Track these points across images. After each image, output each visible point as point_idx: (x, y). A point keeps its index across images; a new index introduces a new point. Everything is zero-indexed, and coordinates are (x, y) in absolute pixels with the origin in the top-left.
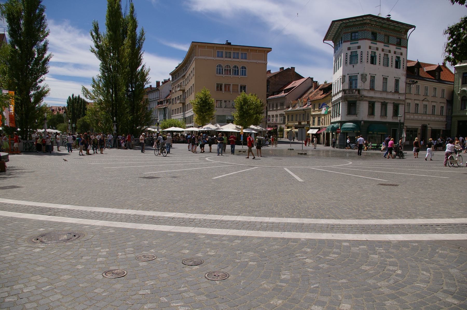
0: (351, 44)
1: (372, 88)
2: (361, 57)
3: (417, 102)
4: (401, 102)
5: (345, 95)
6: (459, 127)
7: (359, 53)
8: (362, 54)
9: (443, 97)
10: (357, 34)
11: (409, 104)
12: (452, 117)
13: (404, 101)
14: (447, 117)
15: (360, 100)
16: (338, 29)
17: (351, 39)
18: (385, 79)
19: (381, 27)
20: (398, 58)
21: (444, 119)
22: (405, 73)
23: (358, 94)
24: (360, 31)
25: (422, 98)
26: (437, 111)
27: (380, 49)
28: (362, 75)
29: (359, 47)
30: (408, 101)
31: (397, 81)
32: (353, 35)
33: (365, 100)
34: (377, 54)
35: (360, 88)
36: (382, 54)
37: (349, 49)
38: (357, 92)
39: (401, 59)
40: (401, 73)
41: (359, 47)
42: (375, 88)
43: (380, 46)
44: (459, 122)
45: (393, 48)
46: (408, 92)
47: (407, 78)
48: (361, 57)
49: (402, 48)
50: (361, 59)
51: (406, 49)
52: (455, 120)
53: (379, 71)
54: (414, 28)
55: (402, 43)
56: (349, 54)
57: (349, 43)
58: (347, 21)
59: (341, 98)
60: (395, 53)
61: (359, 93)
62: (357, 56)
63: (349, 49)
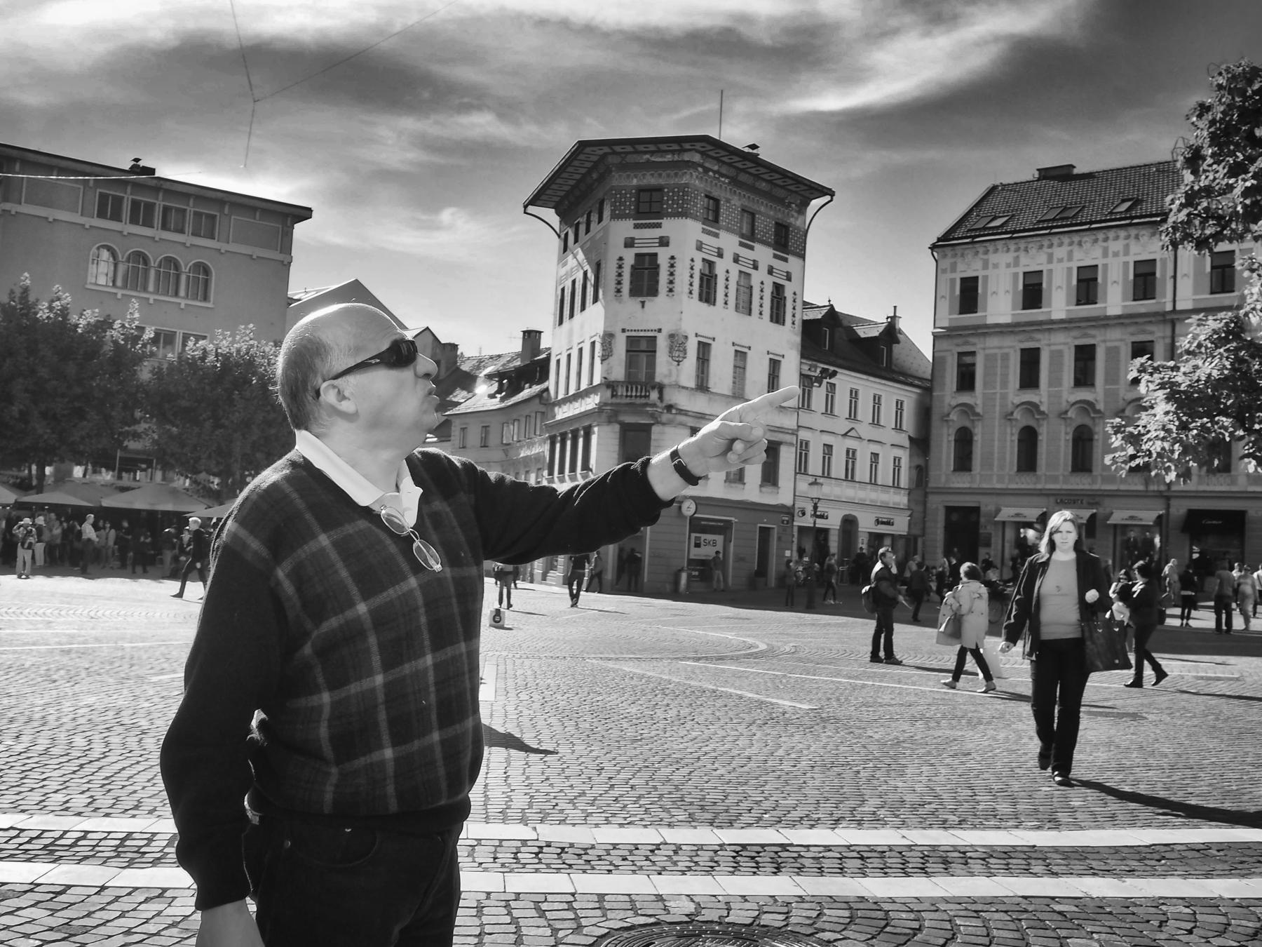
0: (636, 226)
1: (702, 386)
2: (672, 274)
3: (828, 439)
4: (788, 438)
5: (615, 400)
6: (950, 528)
7: (663, 261)
8: (672, 266)
9: (898, 428)
11: (807, 443)
12: (926, 495)
13: (794, 433)
14: (910, 492)
15: (664, 424)
16: (590, 171)
17: (638, 212)
18: (741, 356)
19: (734, 182)
20: (778, 288)
21: (902, 499)
22: (798, 339)
23: (659, 403)
25: (842, 425)
26: (885, 475)
27: (728, 256)
30: (803, 435)
31: (775, 365)
33: (682, 424)
34: (720, 270)
35: (666, 381)
36: (735, 270)
37: (629, 243)
38: (654, 395)
39: (788, 294)
40: (785, 341)
41: (664, 242)
42: (711, 384)
43: (729, 242)
44: (950, 510)
45: (764, 254)
46: (805, 402)
47: (803, 356)
48: (672, 274)
49: (791, 258)
50: (671, 282)
51: (800, 261)
52: (937, 504)
53: (720, 324)
54: (828, 198)
55: (788, 242)
56: (629, 260)
57: (631, 222)
58: (629, 148)
59: (600, 409)
60: (771, 271)
61: (661, 398)
62: (655, 268)
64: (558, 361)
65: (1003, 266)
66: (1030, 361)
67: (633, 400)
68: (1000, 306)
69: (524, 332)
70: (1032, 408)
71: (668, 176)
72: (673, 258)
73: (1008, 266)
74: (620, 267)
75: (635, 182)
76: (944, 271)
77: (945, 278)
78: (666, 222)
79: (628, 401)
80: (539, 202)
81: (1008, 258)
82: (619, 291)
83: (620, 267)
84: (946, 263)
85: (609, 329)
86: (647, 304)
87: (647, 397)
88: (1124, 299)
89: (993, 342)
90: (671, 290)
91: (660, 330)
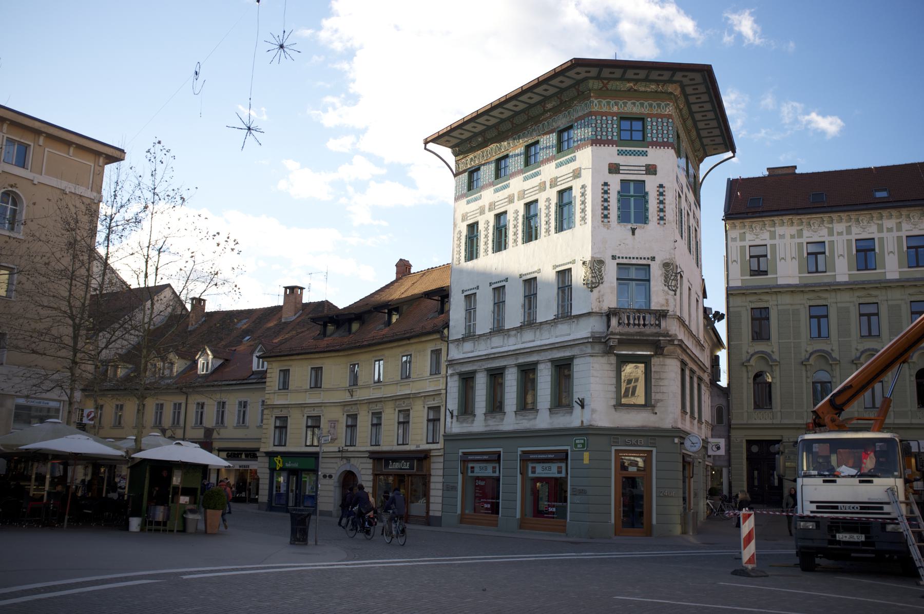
0: (620, 153)
2: (661, 202)
8: (661, 194)
10: (637, 125)
12: (729, 432)
24: (651, 116)
28: (666, 265)
29: (651, 170)
32: (626, 125)
37: (614, 169)
41: (651, 170)
44: (750, 443)
48: (661, 202)
52: (740, 437)
54: (730, 154)
57: (614, 150)
59: (596, 340)
62: (643, 197)
63: (614, 169)
64: (470, 298)
65: (788, 236)
66: (819, 316)
67: (642, 329)
68: (788, 271)
69: (286, 288)
70: (765, 357)
71: (651, 105)
72: (661, 186)
73: (792, 237)
74: (606, 192)
75: (615, 109)
76: (734, 240)
77: (735, 246)
78: (650, 150)
79: (636, 329)
80: (446, 138)
81: (793, 230)
82: (606, 217)
83: (606, 192)
84: (734, 234)
85: (598, 256)
86: (636, 231)
87: (659, 325)
88: (900, 266)
89: (786, 299)
90: (662, 219)
91: (653, 259)
